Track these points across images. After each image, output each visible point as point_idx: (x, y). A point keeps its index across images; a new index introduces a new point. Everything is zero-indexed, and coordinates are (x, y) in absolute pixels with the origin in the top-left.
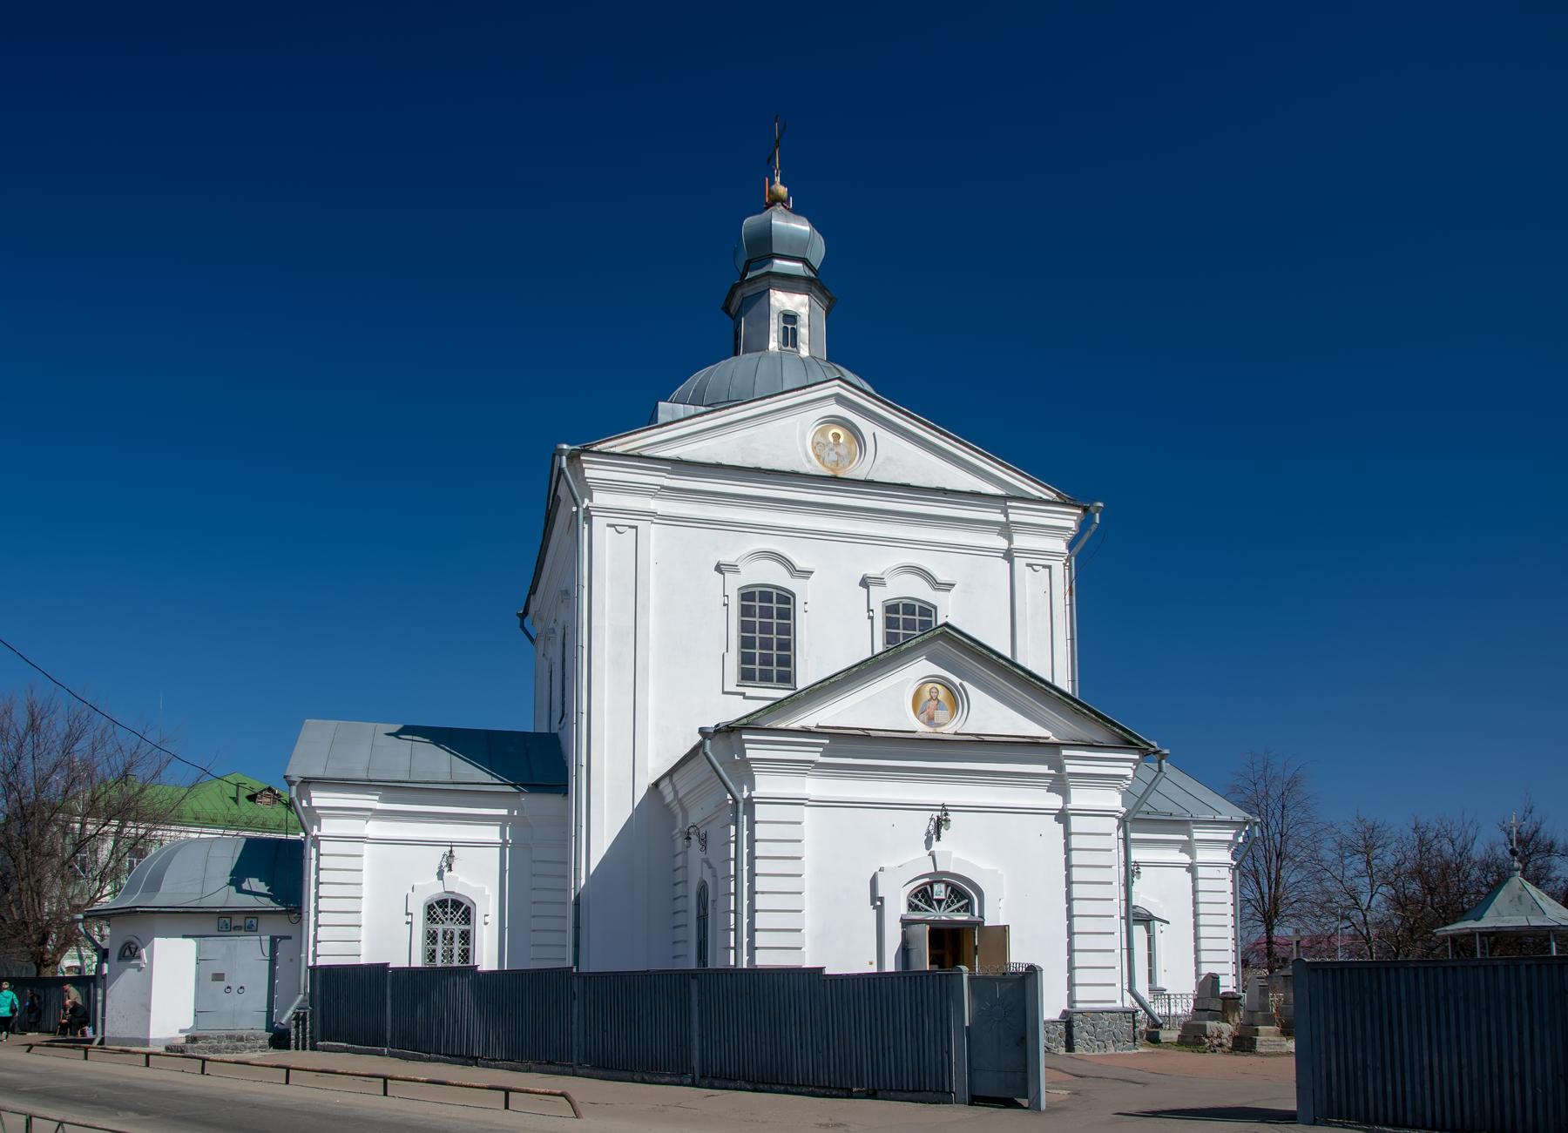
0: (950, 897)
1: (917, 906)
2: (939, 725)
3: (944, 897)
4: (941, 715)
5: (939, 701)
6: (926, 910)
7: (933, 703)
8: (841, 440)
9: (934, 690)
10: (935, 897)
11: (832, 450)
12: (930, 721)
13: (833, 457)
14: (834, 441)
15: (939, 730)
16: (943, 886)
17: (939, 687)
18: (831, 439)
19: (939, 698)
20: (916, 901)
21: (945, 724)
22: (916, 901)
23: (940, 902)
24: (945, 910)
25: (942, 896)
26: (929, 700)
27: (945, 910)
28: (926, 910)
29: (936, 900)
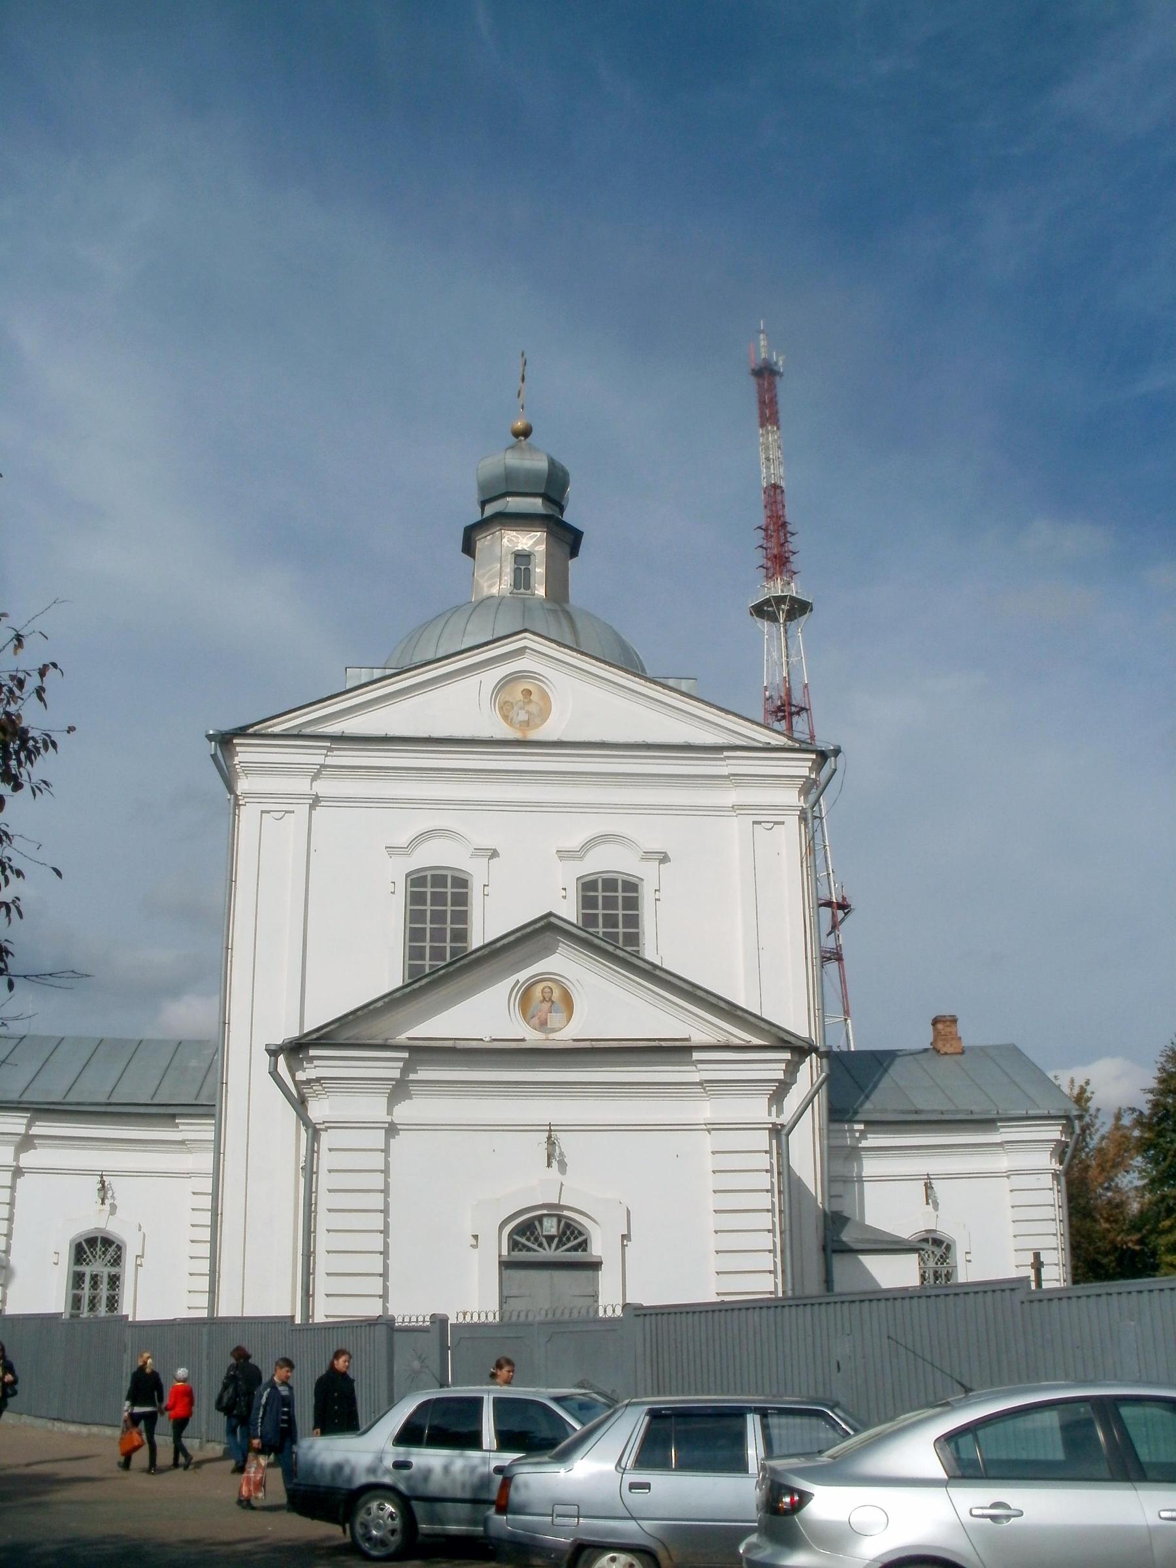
0: (564, 1233)
1: (524, 1246)
2: (554, 1030)
3: (556, 1233)
4: (555, 1019)
5: (553, 1002)
7: (546, 1006)
9: (547, 990)
12: (543, 1025)
13: (523, 716)
16: (555, 1220)
18: (520, 696)
20: (523, 1240)
21: (561, 1029)
22: (523, 1240)
23: (550, 1239)
24: (557, 1248)
27: (557, 1248)
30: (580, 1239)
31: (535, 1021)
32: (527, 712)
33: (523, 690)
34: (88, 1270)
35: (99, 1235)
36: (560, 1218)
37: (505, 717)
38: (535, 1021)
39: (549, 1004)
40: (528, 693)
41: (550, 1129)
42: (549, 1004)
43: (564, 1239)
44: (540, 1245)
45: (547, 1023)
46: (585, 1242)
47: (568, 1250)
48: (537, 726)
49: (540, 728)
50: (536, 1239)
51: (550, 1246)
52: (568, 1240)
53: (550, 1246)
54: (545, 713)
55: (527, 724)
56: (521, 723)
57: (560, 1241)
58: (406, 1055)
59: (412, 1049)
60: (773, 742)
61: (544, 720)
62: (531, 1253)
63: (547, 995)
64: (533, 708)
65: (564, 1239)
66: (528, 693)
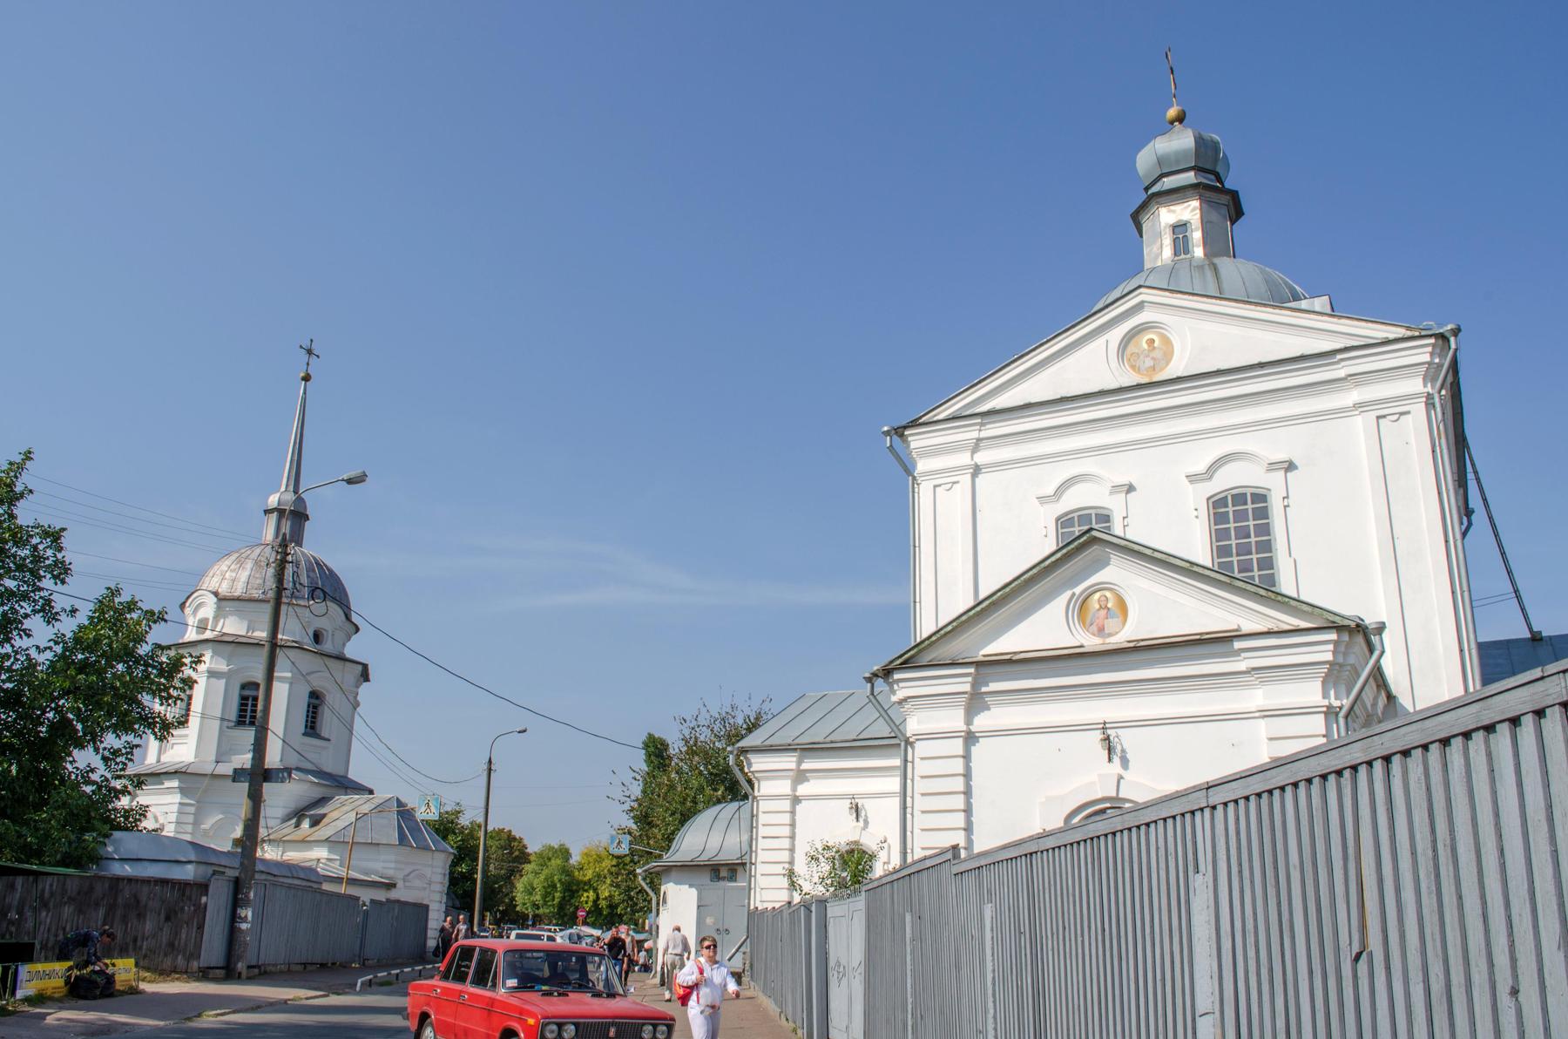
2: (1110, 635)
4: (1111, 625)
5: (1109, 609)
7: (1103, 612)
8: (1156, 344)
9: (1103, 598)
11: (1147, 356)
12: (1101, 631)
13: (1149, 363)
14: (1149, 346)
15: (1108, 640)
18: (1145, 346)
19: (1109, 605)
21: (1117, 633)
26: (1098, 610)
32: (1153, 359)
37: (1133, 367)
38: (1094, 628)
39: (1106, 611)
42: (1106, 611)
54: (1168, 355)
58: (972, 670)
60: (1391, 336)
61: (1168, 363)
63: (1102, 603)
64: (1157, 354)
66: (1151, 341)
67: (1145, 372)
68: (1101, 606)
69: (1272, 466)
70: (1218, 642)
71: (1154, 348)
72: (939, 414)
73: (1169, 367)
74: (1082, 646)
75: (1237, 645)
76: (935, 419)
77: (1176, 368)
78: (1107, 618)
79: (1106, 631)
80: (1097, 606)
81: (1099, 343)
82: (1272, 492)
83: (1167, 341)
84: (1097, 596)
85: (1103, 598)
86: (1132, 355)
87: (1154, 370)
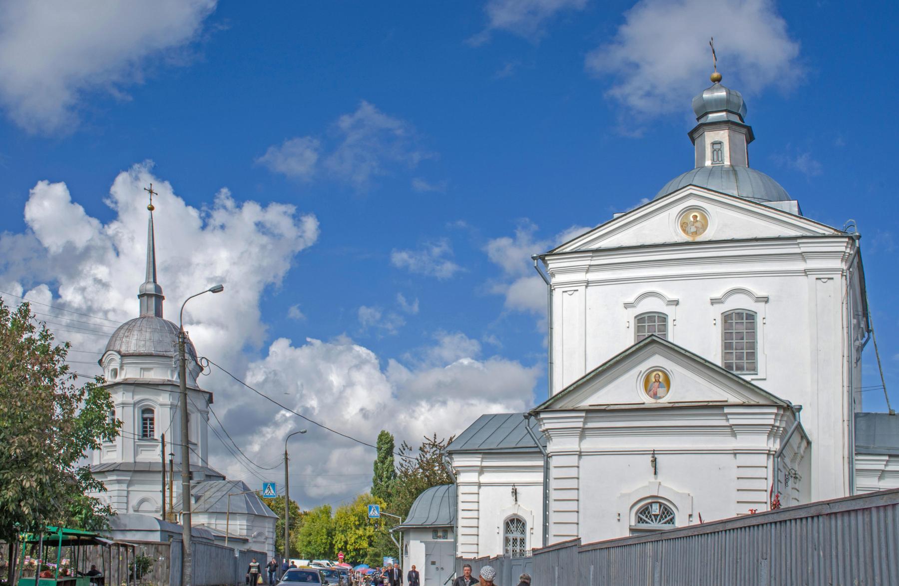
0: (664, 513)
1: (645, 521)
2: (660, 398)
3: (658, 513)
4: (661, 392)
5: (660, 382)
6: (649, 523)
7: (657, 384)
8: (698, 219)
9: (657, 376)
10: (653, 513)
11: (693, 225)
12: (655, 396)
13: (693, 229)
14: (694, 220)
15: (660, 401)
17: (660, 373)
19: (660, 380)
21: (664, 397)
22: (644, 518)
23: (656, 516)
24: (658, 523)
25: (657, 512)
26: (654, 382)
27: (660, 521)
28: (649, 523)
29: (654, 515)
30: (671, 517)
31: (652, 393)
32: (696, 227)
33: (694, 216)
34: (511, 536)
35: (515, 517)
36: (661, 504)
37: (684, 231)
38: (652, 393)
40: (695, 217)
41: (654, 453)
43: (664, 516)
44: (652, 521)
45: (657, 393)
46: (673, 518)
47: (665, 523)
48: (701, 234)
49: (702, 235)
50: (650, 517)
51: (656, 520)
52: (666, 517)
53: (656, 520)
54: (704, 227)
55: (696, 233)
56: (692, 233)
57: (662, 517)
58: (583, 414)
59: (587, 411)
61: (704, 231)
62: (648, 525)
63: (657, 378)
64: (698, 224)
65: (664, 516)
67: (691, 235)
68: (656, 381)
69: (759, 299)
70: (717, 407)
71: (697, 221)
72: (566, 248)
73: (705, 233)
74: (643, 404)
75: (726, 410)
76: (561, 252)
77: (709, 234)
78: (659, 388)
79: (658, 395)
80: (654, 380)
81: (664, 215)
82: (758, 315)
83: (704, 218)
84: (655, 373)
85: (657, 376)
86: (684, 223)
87: (696, 234)
